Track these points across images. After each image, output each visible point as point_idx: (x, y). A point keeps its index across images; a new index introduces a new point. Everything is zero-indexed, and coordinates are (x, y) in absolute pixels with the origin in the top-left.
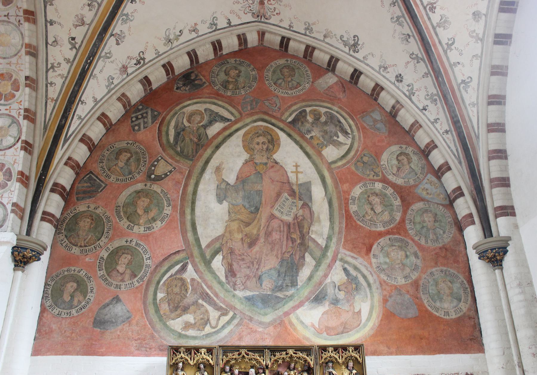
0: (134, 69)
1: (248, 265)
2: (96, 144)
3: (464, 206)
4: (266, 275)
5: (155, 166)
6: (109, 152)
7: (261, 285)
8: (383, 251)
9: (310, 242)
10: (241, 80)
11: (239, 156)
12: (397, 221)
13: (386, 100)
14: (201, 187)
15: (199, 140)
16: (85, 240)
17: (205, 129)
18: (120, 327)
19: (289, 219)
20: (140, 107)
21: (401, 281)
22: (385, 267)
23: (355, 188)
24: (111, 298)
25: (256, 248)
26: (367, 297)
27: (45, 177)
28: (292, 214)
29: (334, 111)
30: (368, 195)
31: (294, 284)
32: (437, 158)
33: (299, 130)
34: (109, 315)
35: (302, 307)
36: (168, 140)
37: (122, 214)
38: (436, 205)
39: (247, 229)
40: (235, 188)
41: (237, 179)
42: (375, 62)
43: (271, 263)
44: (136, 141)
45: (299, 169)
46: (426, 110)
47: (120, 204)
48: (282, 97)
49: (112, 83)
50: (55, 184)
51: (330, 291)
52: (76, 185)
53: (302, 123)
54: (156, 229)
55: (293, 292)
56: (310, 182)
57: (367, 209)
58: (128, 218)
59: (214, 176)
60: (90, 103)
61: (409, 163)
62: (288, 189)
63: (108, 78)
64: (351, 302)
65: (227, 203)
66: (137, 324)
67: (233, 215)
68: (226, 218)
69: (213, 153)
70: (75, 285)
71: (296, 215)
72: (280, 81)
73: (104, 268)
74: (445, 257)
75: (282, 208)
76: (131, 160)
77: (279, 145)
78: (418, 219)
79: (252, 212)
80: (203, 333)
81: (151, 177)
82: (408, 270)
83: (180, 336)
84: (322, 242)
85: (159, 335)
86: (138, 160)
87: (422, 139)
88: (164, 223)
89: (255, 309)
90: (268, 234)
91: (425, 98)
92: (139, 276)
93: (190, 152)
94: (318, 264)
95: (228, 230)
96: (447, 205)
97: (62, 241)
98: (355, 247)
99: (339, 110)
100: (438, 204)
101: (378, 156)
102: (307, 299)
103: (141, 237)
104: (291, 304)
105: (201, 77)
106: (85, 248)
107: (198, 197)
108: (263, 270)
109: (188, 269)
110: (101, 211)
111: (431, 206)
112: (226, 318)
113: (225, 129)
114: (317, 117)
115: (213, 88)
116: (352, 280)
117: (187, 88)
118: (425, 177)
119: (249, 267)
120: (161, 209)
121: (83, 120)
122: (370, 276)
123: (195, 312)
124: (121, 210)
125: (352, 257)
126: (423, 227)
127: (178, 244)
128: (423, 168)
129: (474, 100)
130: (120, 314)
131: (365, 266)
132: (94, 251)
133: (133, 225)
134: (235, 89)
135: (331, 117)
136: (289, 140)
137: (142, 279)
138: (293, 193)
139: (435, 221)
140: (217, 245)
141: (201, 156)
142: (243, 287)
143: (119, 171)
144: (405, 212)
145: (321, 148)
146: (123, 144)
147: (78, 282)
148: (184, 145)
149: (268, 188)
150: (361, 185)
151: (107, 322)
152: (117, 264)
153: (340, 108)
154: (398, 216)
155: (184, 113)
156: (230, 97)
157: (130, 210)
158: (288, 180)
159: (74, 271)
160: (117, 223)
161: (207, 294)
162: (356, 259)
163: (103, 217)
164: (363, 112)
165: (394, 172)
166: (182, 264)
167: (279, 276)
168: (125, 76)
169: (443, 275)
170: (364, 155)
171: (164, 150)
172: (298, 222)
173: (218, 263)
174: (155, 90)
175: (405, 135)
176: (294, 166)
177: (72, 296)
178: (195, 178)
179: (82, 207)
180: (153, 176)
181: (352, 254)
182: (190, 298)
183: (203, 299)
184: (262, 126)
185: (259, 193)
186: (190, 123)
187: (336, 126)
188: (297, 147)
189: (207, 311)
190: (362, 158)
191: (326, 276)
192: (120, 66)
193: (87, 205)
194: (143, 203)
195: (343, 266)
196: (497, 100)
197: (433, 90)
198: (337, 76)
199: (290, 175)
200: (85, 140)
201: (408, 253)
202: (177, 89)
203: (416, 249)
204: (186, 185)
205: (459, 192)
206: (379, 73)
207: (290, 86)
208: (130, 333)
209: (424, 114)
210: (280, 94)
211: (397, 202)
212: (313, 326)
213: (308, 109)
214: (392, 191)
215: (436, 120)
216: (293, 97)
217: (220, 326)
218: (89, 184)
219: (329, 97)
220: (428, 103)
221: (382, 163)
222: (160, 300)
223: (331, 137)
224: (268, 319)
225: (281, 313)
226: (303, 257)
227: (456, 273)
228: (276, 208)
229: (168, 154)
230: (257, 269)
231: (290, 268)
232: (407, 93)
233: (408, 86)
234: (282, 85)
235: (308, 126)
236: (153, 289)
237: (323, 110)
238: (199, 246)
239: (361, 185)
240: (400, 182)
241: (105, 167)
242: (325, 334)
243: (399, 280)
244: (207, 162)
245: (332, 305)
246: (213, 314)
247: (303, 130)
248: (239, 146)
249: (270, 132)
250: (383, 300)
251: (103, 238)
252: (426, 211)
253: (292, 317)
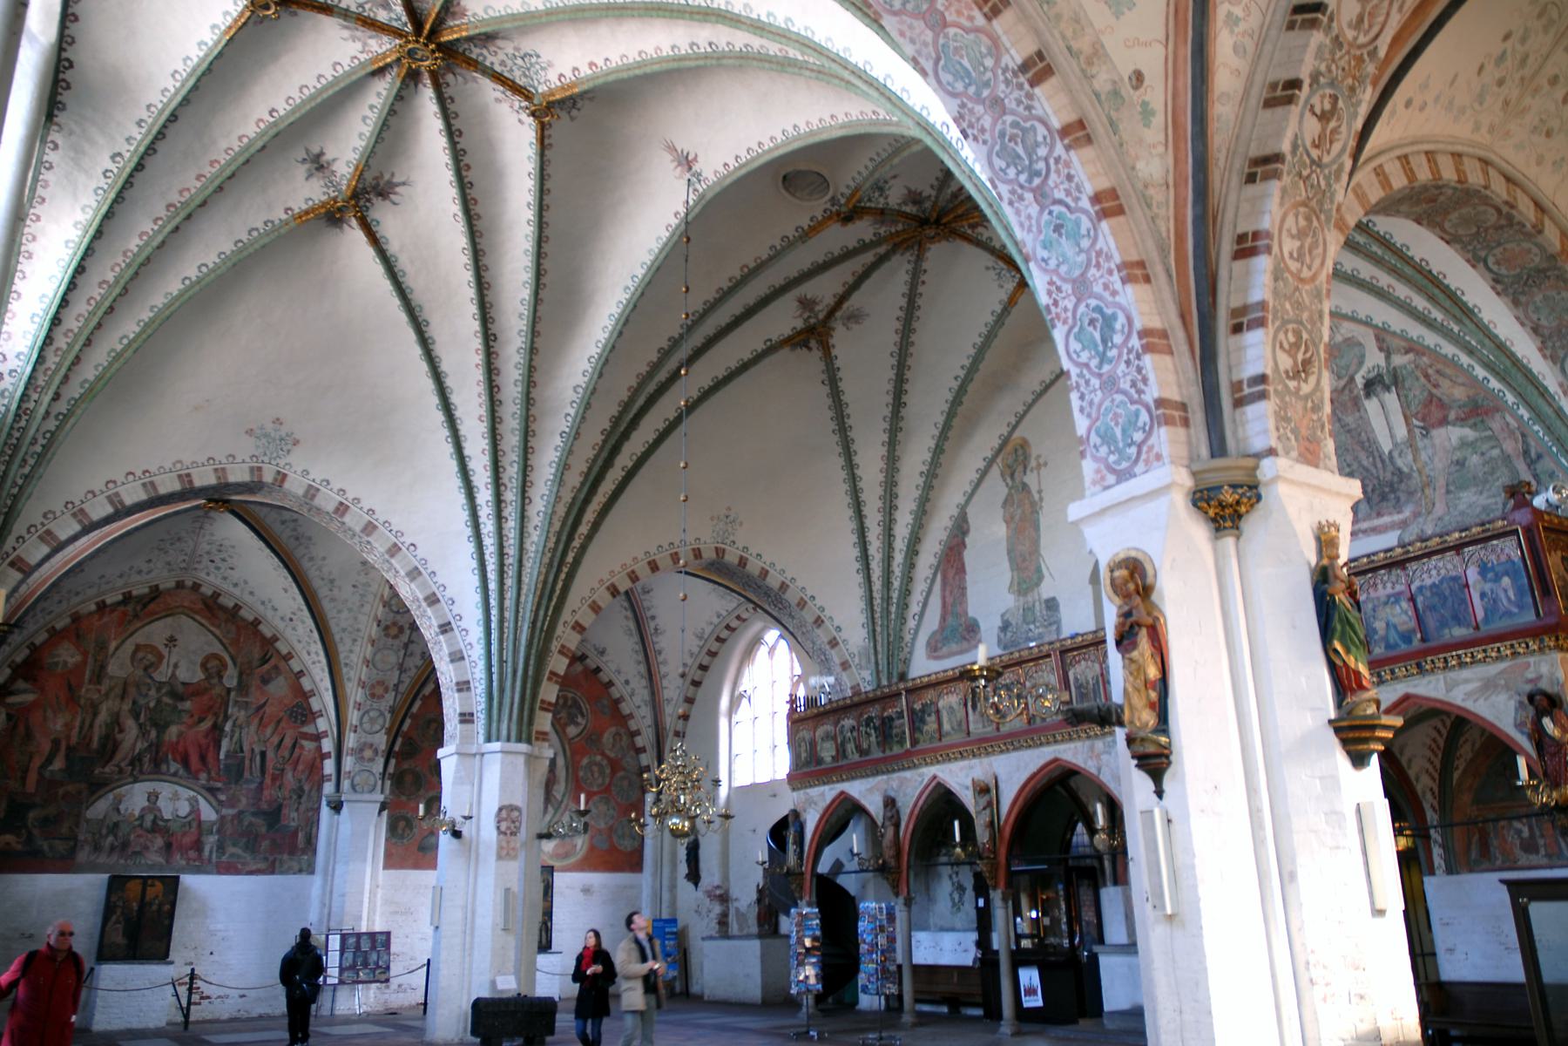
30: (591, 764)
32: (639, 742)
42: (613, 667)
84: (559, 797)
87: (633, 725)
101: (601, 735)
175: (622, 719)
179: (406, 766)
196: (685, 717)
211: (608, 771)
240: (612, 755)
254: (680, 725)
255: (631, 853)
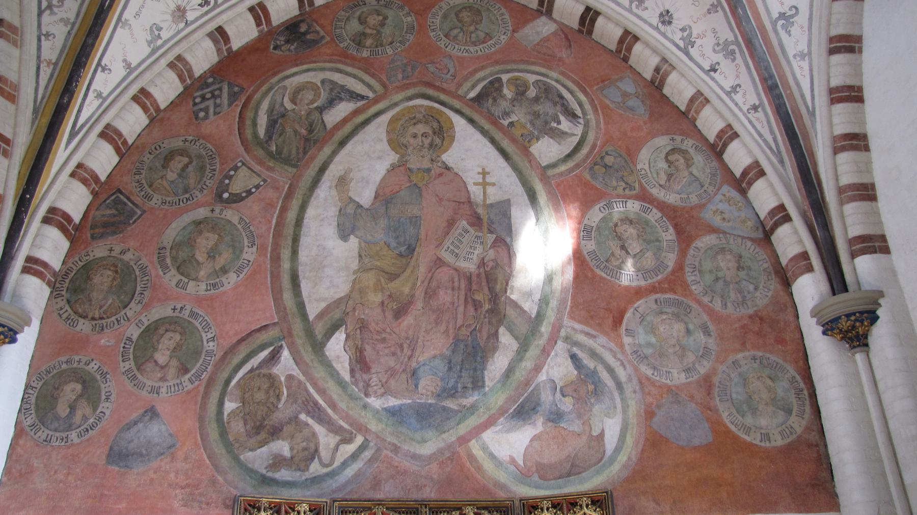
0: (198, 13)
1: (393, 349)
2: (130, 142)
3: (792, 240)
4: (426, 368)
5: (230, 178)
6: (151, 157)
7: (416, 386)
8: (645, 323)
9: (508, 308)
10: (387, 31)
11: (380, 158)
12: (670, 269)
13: (644, 60)
14: (310, 212)
15: (311, 131)
16: (101, 307)
17: (321, 113)
18: (155, 464)
19: (469, 266)
20: (210, 80)
21: (678, 378)
22: (649, 351)
23: (591, 211)
24: (141, 411)
25: (408, 320)
26: (615, 407)
27: (32, 197)
28: (475, 257)
29: (552, 79)
31: (477, 383)
32: (738, 157)
33: (489, 111)
34: (136, 441)
35: (493, 428)
36: (255, 134)
37: (168, 261)
38: (739, 240)
39: (393, 286)
40: (372, 213)
41: (376, 198)
43: (434, 347)
44: (200, 137)
45: (488, 179)
46: (715, 71)
47: (165, 244)
48: (458, 57)
49: (159, 37)
50: (52, 210)
51: (546, 397)
52: (92, 213)
53: (495, 100)
54: (227, 287)
55: (475, 398)
56: (509, 201)
57: (613, 247)
58: (178, 268)
59: (334, 192)
60: (119, 72)
61: (688, 166)
62: (469, 213)
63: (151, 28)
64: (586, 418)
65: (357, 240)
66: (186, 459)
67: (367, 261)
68: (355, 265)
69: (334, 153)
70: (79, 387)
71: (483, 259)
72: (455, 32)
73: (131, 356)
74: (759, 334)
75: (458, 247)
76: (190, 169)
77: (452, 138)
78: (707, 265)
79: (401, 255)
80: (307, 475)
81: (224, 197)
82: (691, 357)
83: (265, 481)
85: (225, 480)
86: (202, 169)
87: (710, 123)
88: (241, 276)
89: (404, 430)
90: (430, 294)
91: (714, 50)
92: (193, 372)
93: (294, 152)
94: (524, 347)
95: (358, 289)
96: (761, 239)
97: (61, 309)
98: (592, 317)
99: (561, 78)
100: (743, 238)
101: (631, 155)
102: (502, 412)
103: (199, 300)
104: (472, 421)
105: (318, 28)
106: (100, 322)
107: (304, 230)
108: (421, 359)
109: (282, 358)
110: (132, 257)
111: (731, 242)
112: (350, 448)
113: (356, 113)
114: (521, 90)
115: (337, 45)
116: (587, 375)
117: (293, 47)
118: (718, 190)
119: (394, 354)
120: (237, 250)
121: (105, 99)
122: (621, 368)
123: (292, 437)
124: (168, 254)
125: (587, 334)
126: (717, 279)
127: (266, 312)
128: (714, 175)
129: (803, 47)
130: (156, 440)
131: (611, 350)
132: (116, 326)
133: (186, 280)
134: (377, 47)
135: (546, 89)
136: (470, 129)
137: (198, 376)
138: (476, 221)
139: (740, 268)
140: (337, 315)
141: (313, 158)
142: (383, 390)
143: (168, 188)
144: (683, 253)
145: (529, 142)
146: (178, 143)
147: (84, 383)
148: (284, 142)
149: (432, 213)
150: (602, 205)
151: (133, 455)
152: (155, 349)
153: (563, 74)
154: (671, 260)
155: (285, 88)
156: (365, 60)
157: (183, 255)
158: (469, 197)
159: (79, 362)
160: (158, 276)
161: (316, 404)
162: (595, 337)
163: (135, 267)
164: (603, 81)
165: (662, 183)
166: (272, 348)
167: (450, 369)
168: (182, 25)
169: (756, 365)
170: (607, 154)
171: (247, 150)
172: (485, 271)
173: (337, 347)
174: (237, 51)
176: (479, 173)
177: (73, 408)
178: (300, 197)
179: (99, 251)
180: (226, 195)
181: (587, 329)
182: (284, 409)
183: (308, 413)
184: (422, 106)
185: (415, 221)
186: (295, 104)
187: (555, 104)
188: (485, 142)
189: (314, 434)
190: (602, 158)
191: (537, 369)
192: (173, 7)
193: (109, 247)
194: (206, 241)
195: (569, 351)
197: (727, 34)
198: (555, 21)
199: (472, 188)
200: (110, 134)
201: (691, 327)
202: (275, 48)
203: (705, 318)
204: (284, 210)
205: (781, 215)
206: (630, 10)
207: (473, 39)
208: (172, 475)
209: (713, 79)
210: (455, 53)
211: (669, 235)
212: (513, 461)
213: (505, 77)
214: (659, 215)
215: (735, 89)
216: (478, 58)
217: (337, 464)
218: (114, 211)
219: (543, 56)
220: (719, 57)
221: (639, 167)
222: (229, 415)
223: (546, 123)
224: (426, 450)
225: (453, 439)
226: (496, 335)
227: (780, 361)
228: (446, 247)
229: (254, 158)
230: (410, 358)
231: (471, 356)
232: (681, 44)
233: (683, 30)
234: (460, 38)
235: (504, 105)
236: (218, 394)
237: (531, 78)
238: (304, 315)
239: (602, 205)
240: (672, 198)
241: (143, 181)
242: (536, 477)
243: (675, 375)
244: (323, 169)
245: (550, 424)
246: (326, 439)
247: (497, 111)
248: (381, 140)
249: (437, 116)
250: (646, 412)
251: (132, 305)
252: (722, 250)
253: (474, 447)
254: (839, 70)
255: (788, 450)
